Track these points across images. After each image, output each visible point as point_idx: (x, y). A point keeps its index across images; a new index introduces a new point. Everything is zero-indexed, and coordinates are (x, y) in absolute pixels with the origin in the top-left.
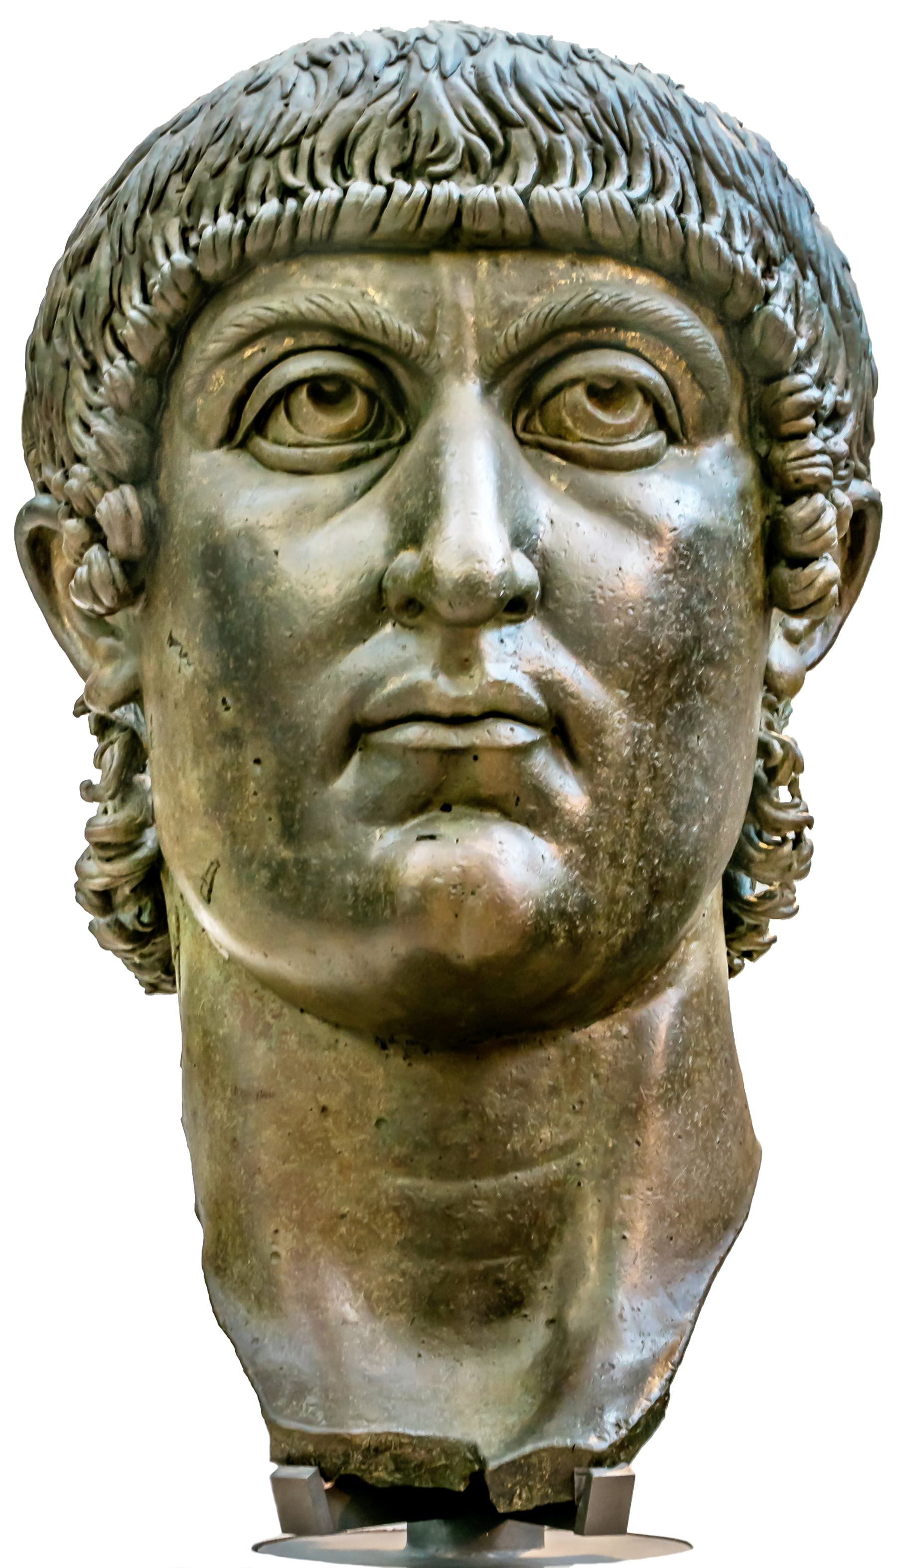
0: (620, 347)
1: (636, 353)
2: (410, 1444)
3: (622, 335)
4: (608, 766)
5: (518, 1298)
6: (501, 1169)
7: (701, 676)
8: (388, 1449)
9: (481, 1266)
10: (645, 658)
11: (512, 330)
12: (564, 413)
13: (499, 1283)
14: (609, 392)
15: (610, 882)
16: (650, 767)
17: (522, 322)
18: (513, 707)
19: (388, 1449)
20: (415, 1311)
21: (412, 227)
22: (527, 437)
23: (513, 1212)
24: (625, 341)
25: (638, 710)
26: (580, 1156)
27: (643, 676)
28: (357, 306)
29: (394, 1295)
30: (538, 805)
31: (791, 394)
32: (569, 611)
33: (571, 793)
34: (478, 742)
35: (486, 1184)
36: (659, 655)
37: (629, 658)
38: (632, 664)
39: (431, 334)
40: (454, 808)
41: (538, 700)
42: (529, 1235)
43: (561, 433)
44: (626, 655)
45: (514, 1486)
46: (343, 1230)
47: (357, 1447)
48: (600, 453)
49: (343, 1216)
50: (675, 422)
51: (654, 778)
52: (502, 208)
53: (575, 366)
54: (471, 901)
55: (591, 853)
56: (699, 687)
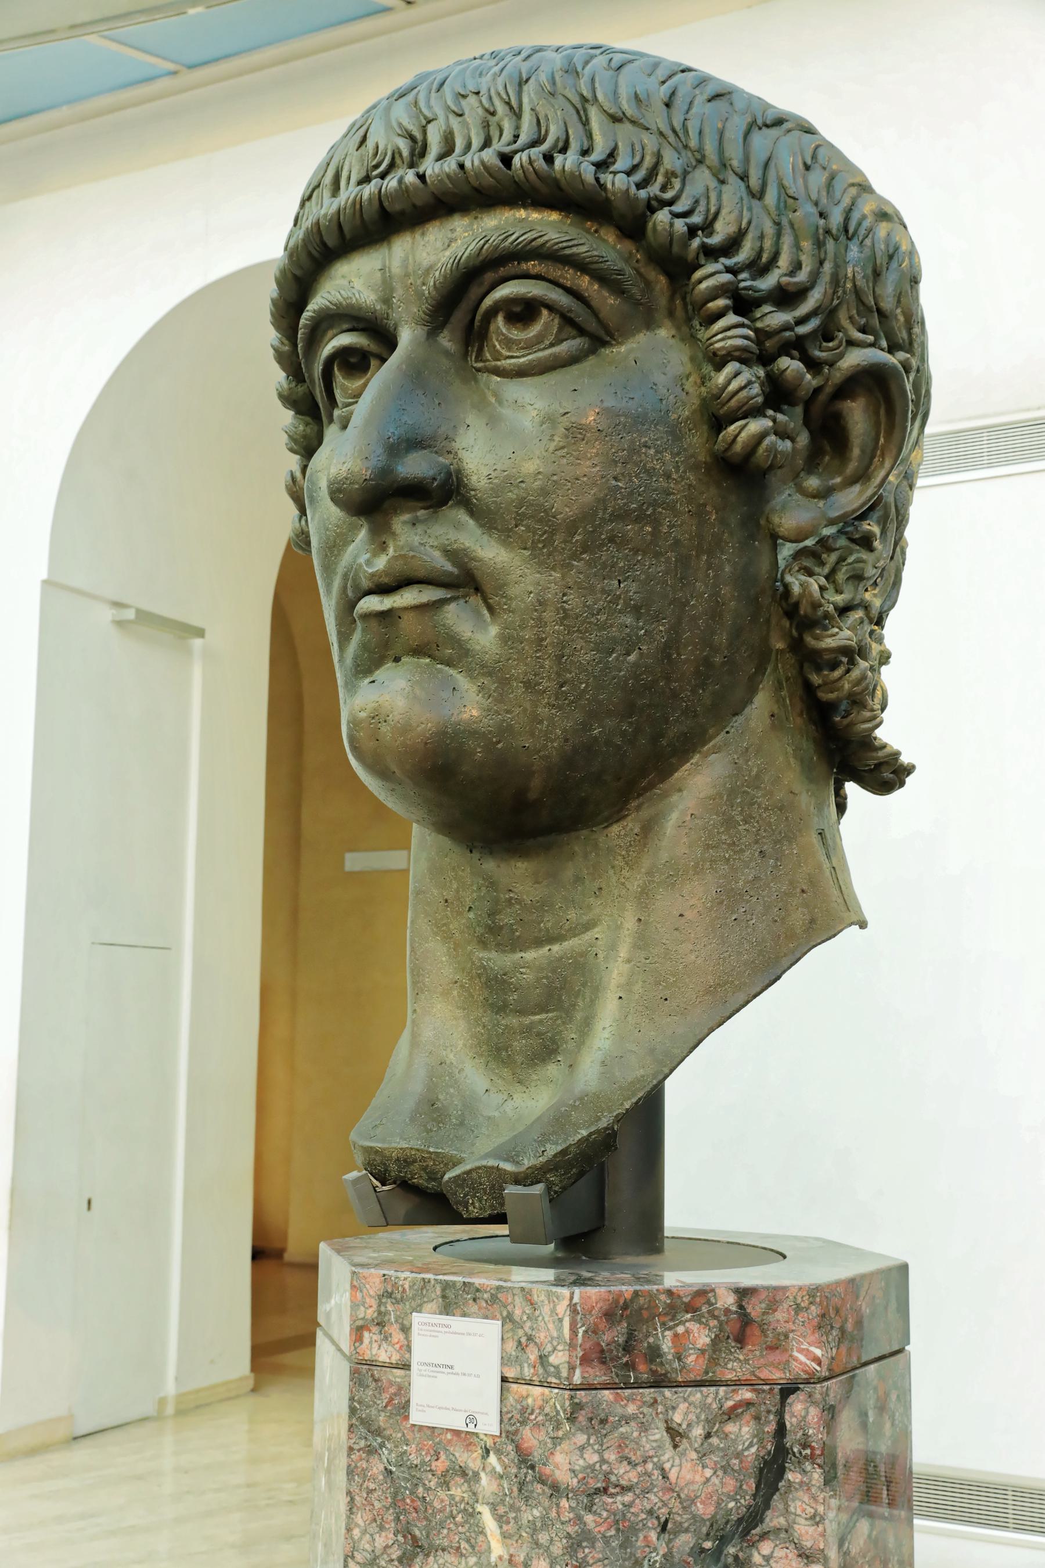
0: (526, 276)
1: (538, 277)
2: (430, 1158)
3: (524, 266)
4: (512, 612)
5: (555, 1047)
6: (538, 943)
7: (612, 530)
8: (415, 1161)
9: (527, 1020)
10: (540, 521)
11: (432, 284)
12: (494, 340)
13: (539, 1034)
14: (523, 312)
15: (528, 705)
16: (557, 609)
17: (437, 273)
18: (421, 573)
19: (415, 1161)
20: (490, 1056)
21: (358, 221)
22: (479, 365)
23: (547, 978)
24: (528, 269)
25: (540, 564)
26: (598, 932)
27: (541, 536)
28: (342, 292)
29: (479, 1043)
30: (453, 649)
31: (700, 281)
32: (473, 493)
33: (484, 636)
34: (395, 605)
35: (530, 955)
36: (554, 517)
37: (525, 523)
38: (528, 527)
39: (387, 301)
40: (403, 659)
41: (449, 567)
42: (560, 996)
43: (497, 356)
44: (522, 521)
45: (466, 1195)
46: (455, 993)
47: (390, 1158)
48: (514, 365)
49: (456, 982)
50: (592, 326)
51: (564, 618)
52: (403, 189)
53: (488, 301)
54: (384, 728)
55: (504, 682)
56: (612, 540)
